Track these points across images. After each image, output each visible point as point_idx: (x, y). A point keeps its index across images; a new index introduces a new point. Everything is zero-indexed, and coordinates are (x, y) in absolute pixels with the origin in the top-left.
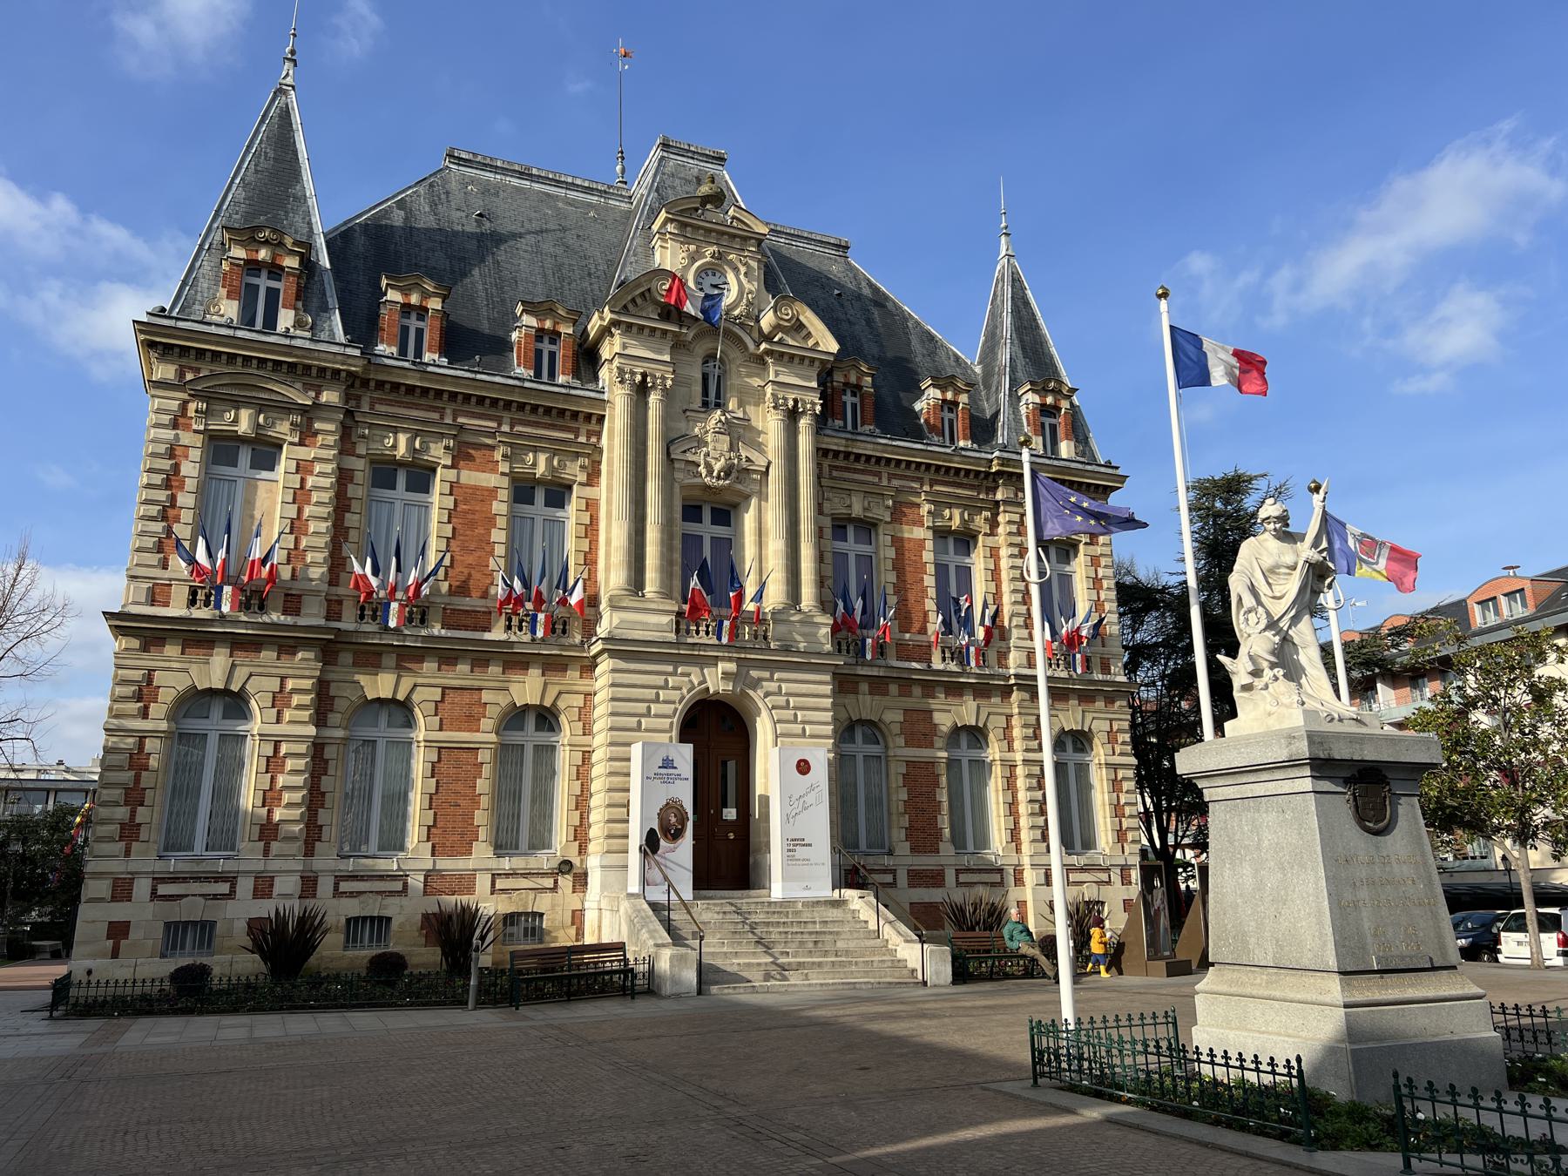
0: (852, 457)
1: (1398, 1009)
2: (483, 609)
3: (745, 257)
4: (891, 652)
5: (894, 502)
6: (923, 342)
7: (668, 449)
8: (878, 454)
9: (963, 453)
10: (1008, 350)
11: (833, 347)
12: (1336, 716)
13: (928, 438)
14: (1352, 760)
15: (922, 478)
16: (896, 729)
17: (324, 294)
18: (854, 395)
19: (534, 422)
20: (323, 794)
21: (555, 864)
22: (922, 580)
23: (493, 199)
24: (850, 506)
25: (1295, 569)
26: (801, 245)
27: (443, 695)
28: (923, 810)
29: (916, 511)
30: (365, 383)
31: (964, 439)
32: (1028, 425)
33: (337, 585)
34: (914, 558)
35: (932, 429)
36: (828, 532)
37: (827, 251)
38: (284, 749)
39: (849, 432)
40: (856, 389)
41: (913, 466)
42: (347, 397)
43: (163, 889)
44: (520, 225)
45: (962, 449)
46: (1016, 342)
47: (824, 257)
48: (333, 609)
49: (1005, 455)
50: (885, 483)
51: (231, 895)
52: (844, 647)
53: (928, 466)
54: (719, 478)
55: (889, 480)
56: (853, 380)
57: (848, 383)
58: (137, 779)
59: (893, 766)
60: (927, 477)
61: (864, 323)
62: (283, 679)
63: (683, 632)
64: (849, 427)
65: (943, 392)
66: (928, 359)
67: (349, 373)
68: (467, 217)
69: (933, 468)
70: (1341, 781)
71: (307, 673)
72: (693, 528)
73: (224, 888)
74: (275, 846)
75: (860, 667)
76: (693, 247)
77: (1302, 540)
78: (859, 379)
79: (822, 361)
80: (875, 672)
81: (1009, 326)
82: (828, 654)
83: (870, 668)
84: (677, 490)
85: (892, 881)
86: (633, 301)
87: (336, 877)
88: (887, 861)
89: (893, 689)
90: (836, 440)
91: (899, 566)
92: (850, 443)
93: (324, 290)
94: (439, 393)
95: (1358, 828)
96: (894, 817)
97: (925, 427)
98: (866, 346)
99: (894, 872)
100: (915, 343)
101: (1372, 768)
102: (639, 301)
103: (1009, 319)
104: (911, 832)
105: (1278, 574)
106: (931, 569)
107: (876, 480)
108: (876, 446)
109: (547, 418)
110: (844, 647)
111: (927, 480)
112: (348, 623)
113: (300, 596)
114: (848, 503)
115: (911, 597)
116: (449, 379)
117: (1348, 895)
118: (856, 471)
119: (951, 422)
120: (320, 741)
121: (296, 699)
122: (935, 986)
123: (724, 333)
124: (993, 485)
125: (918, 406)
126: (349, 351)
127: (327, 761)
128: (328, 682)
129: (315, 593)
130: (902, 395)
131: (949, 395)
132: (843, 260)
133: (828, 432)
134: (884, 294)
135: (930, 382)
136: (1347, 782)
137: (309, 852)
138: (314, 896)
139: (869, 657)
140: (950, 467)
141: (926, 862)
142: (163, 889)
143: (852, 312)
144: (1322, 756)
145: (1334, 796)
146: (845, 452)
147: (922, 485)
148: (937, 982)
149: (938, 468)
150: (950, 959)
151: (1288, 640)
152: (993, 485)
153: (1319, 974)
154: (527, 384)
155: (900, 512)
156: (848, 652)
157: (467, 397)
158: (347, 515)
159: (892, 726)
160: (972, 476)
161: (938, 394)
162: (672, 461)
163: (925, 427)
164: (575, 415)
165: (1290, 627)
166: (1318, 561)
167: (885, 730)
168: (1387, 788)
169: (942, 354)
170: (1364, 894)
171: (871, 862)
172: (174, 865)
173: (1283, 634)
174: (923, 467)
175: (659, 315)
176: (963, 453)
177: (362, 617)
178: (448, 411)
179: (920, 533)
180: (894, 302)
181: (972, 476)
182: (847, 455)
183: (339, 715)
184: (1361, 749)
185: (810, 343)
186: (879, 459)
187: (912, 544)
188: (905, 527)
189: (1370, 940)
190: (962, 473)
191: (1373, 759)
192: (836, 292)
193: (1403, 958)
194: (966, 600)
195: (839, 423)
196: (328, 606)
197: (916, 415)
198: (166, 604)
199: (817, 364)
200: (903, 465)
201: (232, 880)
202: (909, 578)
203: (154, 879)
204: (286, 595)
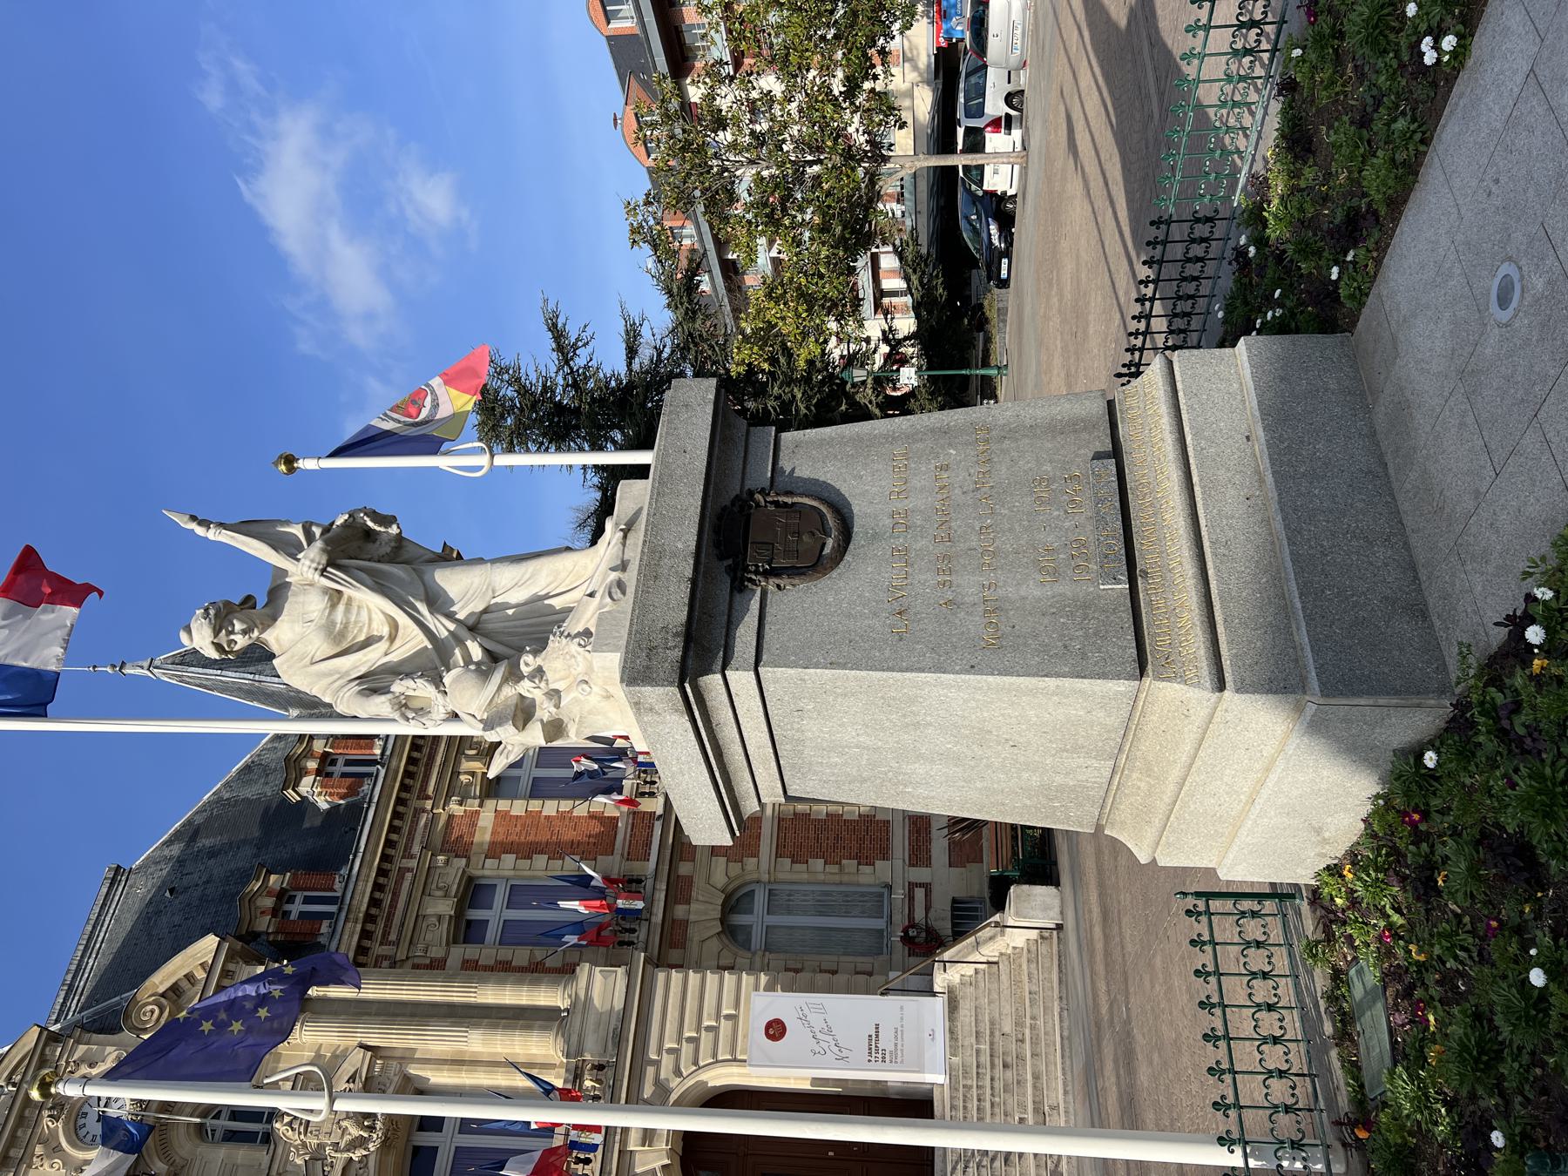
0: (373, 911)
1: (1215, 554)
3: (67, 1063)
4: (636, 868)
5: (442, 852)
6: (249, 782)
8: (373, 875)
9: (388, 753)
10: (268, 679)
11: (211, 941)
12: (614, 576)
13: (364, 798)
14: (694, 581)
15: (415, 809)
16: (735, 869)
18: (291, 900)
22: (547, 818)
24: (440, 918)
25: (339, 592)
26: (102, 934)
28: (837, 838)
29: (456, 822)
31: (371, 748)
35: (352, 791)
36: (471, 951)
37: (117, 898)
39: (340, 909)
40: (283, 896)
41: (397, 823)
45: (383, 754)
46: (260, 668)
47: (124, 903)
50: (413, 863)
52: (627, 937)
53: (400, 801)
55: (411, 857)
56: (269, 902)
57: (273, 908)
59: (781, 876)
60: (415, 803)
61: (212, 861)
64: (333, 908)
65: (307, 773)
66: (271, 777)
69: (404, 795)
70: (738, 597)
75: (654, 919)
76: (39, 1150)
77: (285, 573)
78: (270, 894)
79: (231, 957)
80: (661, 896)
81: (238, 675)
82: (629, 974)
83: (656, 903)
85: (923, 890)
88: (899, 894)
89: (684, 869)
90: (346, 937)
91: (527, 851)
92: (351, 916)
95: (834, 574)
96: (846, 878)
97: (350, 799)
98: (240, 864)
99: (912, 886)
100: (249, 792)
101: (717, 530)
103: (230, 674)
104: (865, 859)
105: (346, 626)
106: (535, 805)
107: (409, 876)
108: (362, 877)
110: (627, 937)
111: (418, 804)
114: (434, 920)
115: (569, 835)
117: (974, 623)
118: (393, 905)
119: (348, 763)
122: (1062, 913)
125: (323, 804)
130: (306, 825)
131: (312, 765)
132: (132, 876)
134: (183, 825)
135: (290, 791)
136: (739, 585)
139: (640, 905)
140: (405, 771)
141: (900, 840)
143: (196, 876)
144: (678, 653)
145: (768, 619)
146: (365, 922)
147: (424, 810)
148: (1057, 910)
149: (404, 788)
150: (1026, 887)
151: (478, 622)
155: (457, 847)
156: (633, 931)
159: (732, 874)
161: (307, 781)
163: (350, 799)
165: (450, 616)
166: (324, 550)
167: (737, 883)
168: (758, 497)
169: (268, 757)
170: (969, 585)
171: (900, 920)
173: (463, 633)
174: (401, 809)
176: (388, 753)
179: (487, 819)
180: (197, 813)
182: (369, 918)
184: (674, 555)
185: (201, 975)
186: (382, 872)
187: (499, 830)
188: (476, 839)
189: (1064, 588)
190: (415, 754)
191: (694, 530)
192: (167, 894)
193: (1100, 520)
194: (577, 761)
195: (325, 927)
197: (335, 809)
199: (231, 967)
200: (394, 837)
202: (543, 836)
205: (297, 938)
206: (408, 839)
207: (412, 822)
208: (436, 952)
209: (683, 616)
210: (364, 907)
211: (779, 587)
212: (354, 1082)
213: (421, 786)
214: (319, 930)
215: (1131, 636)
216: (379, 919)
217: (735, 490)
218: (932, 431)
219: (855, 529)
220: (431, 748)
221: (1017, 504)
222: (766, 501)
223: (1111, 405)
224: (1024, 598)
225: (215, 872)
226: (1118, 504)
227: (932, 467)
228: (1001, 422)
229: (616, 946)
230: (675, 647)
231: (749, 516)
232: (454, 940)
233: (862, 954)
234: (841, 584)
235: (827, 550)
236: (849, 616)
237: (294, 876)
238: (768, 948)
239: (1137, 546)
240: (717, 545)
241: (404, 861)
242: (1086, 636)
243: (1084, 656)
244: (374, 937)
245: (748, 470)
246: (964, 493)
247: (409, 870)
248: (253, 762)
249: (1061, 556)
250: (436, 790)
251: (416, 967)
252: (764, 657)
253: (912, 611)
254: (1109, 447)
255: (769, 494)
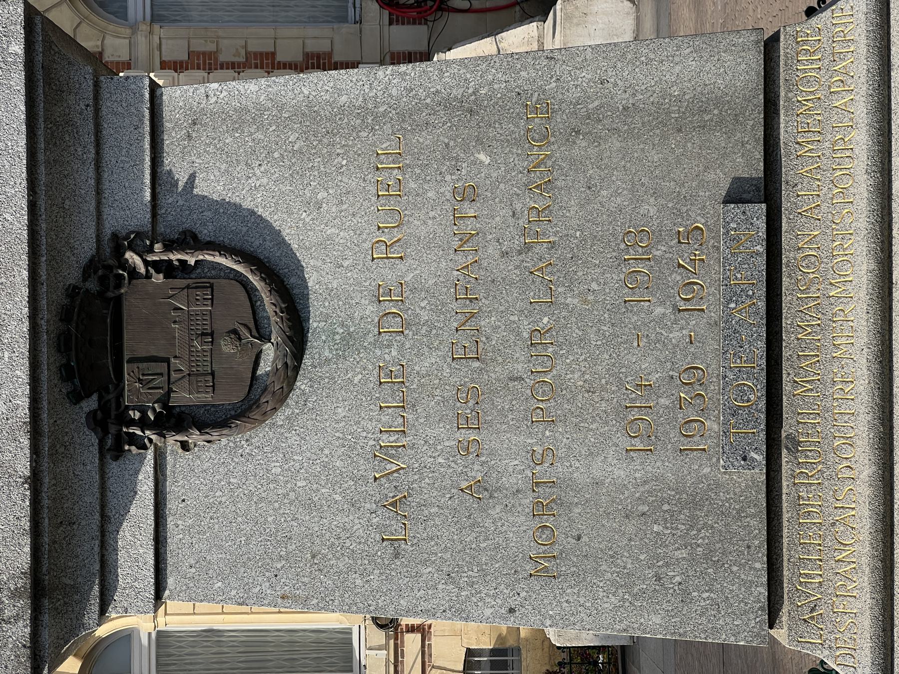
14: (35, 481)
21: (378, 636)
70: (114, 467)
95: (280, 417)
101: (63, 343)
144: (21, 630)
145: (172, 505)
153: (757, 396)
191: (22, 374)
209: (23, 557)
211: (185, 446)
215: (761, 565)
217: (86, 248)
218: (447, 104)
219: (313, 324)
221: (594, 286)
222: (146, 263)
223: (771, 46)
224: (597, 483)
226: (762, 305)
227: (447, 190)
228: (576, 94)
230: (17, 618)
231: (118, 301)
233: (314, 20)
234: (293, 439)
235: (265, 367)
236: (310, 506)
238: (156, 18)
239: (787, 387)
240: (66, 373)
242: (692, 560)
243: (685, 597)
245: (106, 185)
246: (504, 254)
249: (662, 401)
252: (171, 581)
253: (414, 500)
254: (757, 170)
255: (151, 250)
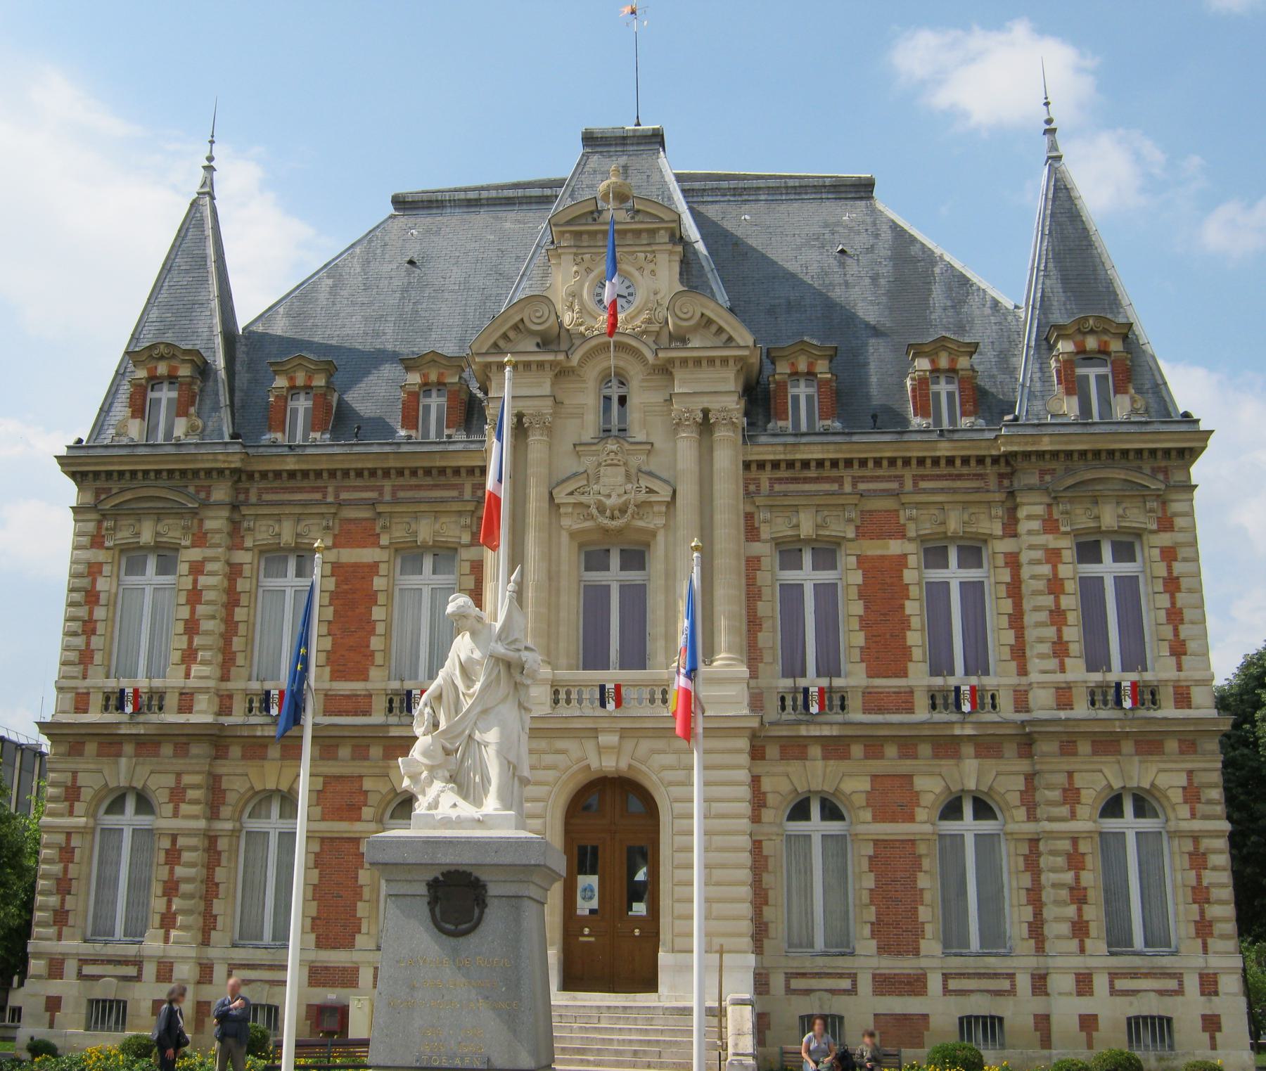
2: (364, 693)
7: (551, 494)
15: (902, 476)
16: (860, 800)
17: (217, 394)
19: (416, 486)
20: (217, 885)
22: (902, 607)
23: (436, 239)
24: (797, 526)
27: (325, 783)
30: (251, 476)
32: (1059, 382)
33: (228, 680)
34: (889, 581)
38: (181, 842)
42: (237, 491)
43: (88, 970)
44: (453, 261)
46: (1053, 273)
48: (225, 709)
49: (1014, 430)
51: (138, 978)
54: (612, 518)
55: (854, 485)
56: (802, 367)
58: (66, 870)
60: (908, 474)
61: (868, 281)
62: (179, 775)
63: (562, 703)
66: (950, 312)
67: (234, 471)
68: (398, 267)
71: (197, 768)
72: (596, 577)
73: (131, 971)
74: (173, 933)
78: (811, 365)
79: (738, 359)
80: (826, 731)
83: (818, 727)
84: (565, 538)
85: (849, 987)
86: (505, 336)
87: (229, 964)
89: (857, 750)
92: (789, 448)
93: (218, 391)
94: (319, 474)
100: (938, 295)
102: (512, 335)
107: (835, 487)
108: (826, 447)
109: (428, 479)
112: (237, 718)
113: (192, 694)
114: (794, 521)
116: (324, 458)
118: (806, 480)
120: (212, 834)
121: (191, 794)
123: (615, 347)
124: (1008, 470)
126: (231, 449)
127: (219, 853)
128: (220, 776)
129: (205, 690)
133: (763, 439)
137: (206, 942)
138: (211, 982)
142: (88, 970)
152: (1008, 470)
154: (405, 449)
157: (346, 473)
158: (237, 610)
159: (854, 797)
160: (973, 463)
162: (558, 506)
164: (457, 471)
172: (97, 949)
175: (538, 345)
177: (250, 710)
178: (330, 490)
181: (973, 463)
182: (791, 464)
183: (230, 808)
186: (835, 463)
192: (840, 248)
196: (221, 702)
198: (86, 711)
199: (731, 362)
200: (871, 464)
201: (138, 962)
203: (80, 960)
204: (181, 694)
205: (772, 401)
206: (872, 477)
207: (890, 477)
208: (765, 532)
210: (798, 456)
212: (647, 492)
213: (927, 476)
214: (780, 420)
216: (792, 471)
220: (969, 475)
225: (857, 289)
229: (780, 695)
232: (778, 543)
237: (828, 381)
241: (849, 479)
244: (776, 471)
247: (841, 485)
248: (972, 285)
250: (925, 491)
251: (749, 517)
